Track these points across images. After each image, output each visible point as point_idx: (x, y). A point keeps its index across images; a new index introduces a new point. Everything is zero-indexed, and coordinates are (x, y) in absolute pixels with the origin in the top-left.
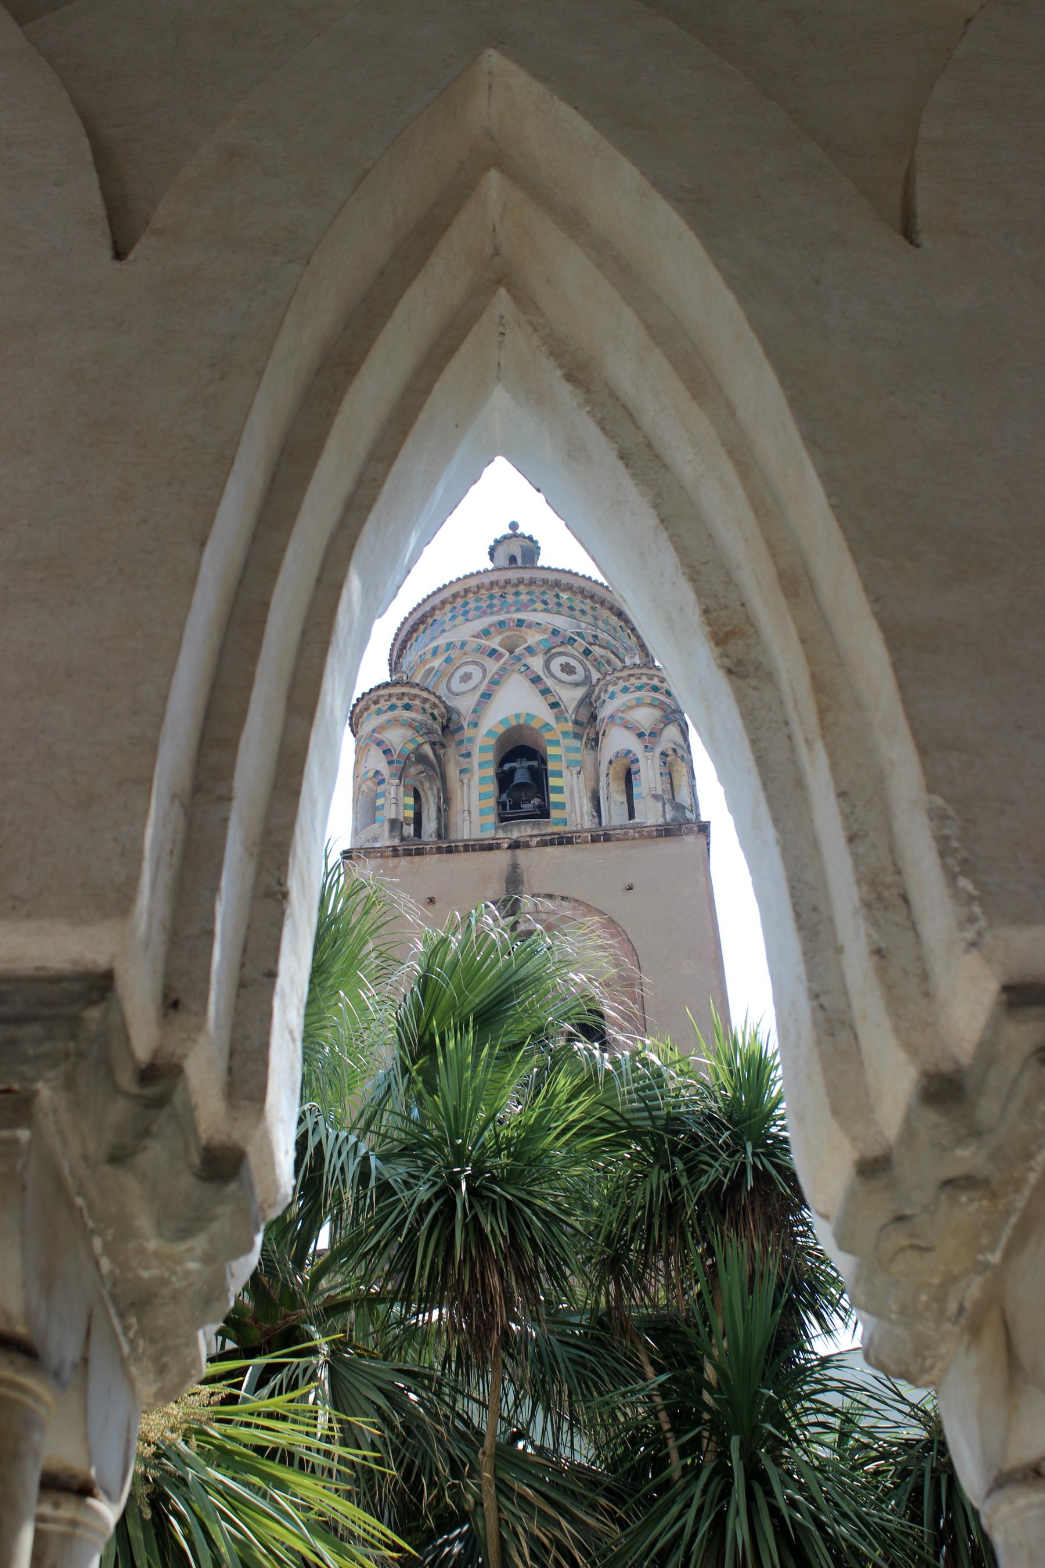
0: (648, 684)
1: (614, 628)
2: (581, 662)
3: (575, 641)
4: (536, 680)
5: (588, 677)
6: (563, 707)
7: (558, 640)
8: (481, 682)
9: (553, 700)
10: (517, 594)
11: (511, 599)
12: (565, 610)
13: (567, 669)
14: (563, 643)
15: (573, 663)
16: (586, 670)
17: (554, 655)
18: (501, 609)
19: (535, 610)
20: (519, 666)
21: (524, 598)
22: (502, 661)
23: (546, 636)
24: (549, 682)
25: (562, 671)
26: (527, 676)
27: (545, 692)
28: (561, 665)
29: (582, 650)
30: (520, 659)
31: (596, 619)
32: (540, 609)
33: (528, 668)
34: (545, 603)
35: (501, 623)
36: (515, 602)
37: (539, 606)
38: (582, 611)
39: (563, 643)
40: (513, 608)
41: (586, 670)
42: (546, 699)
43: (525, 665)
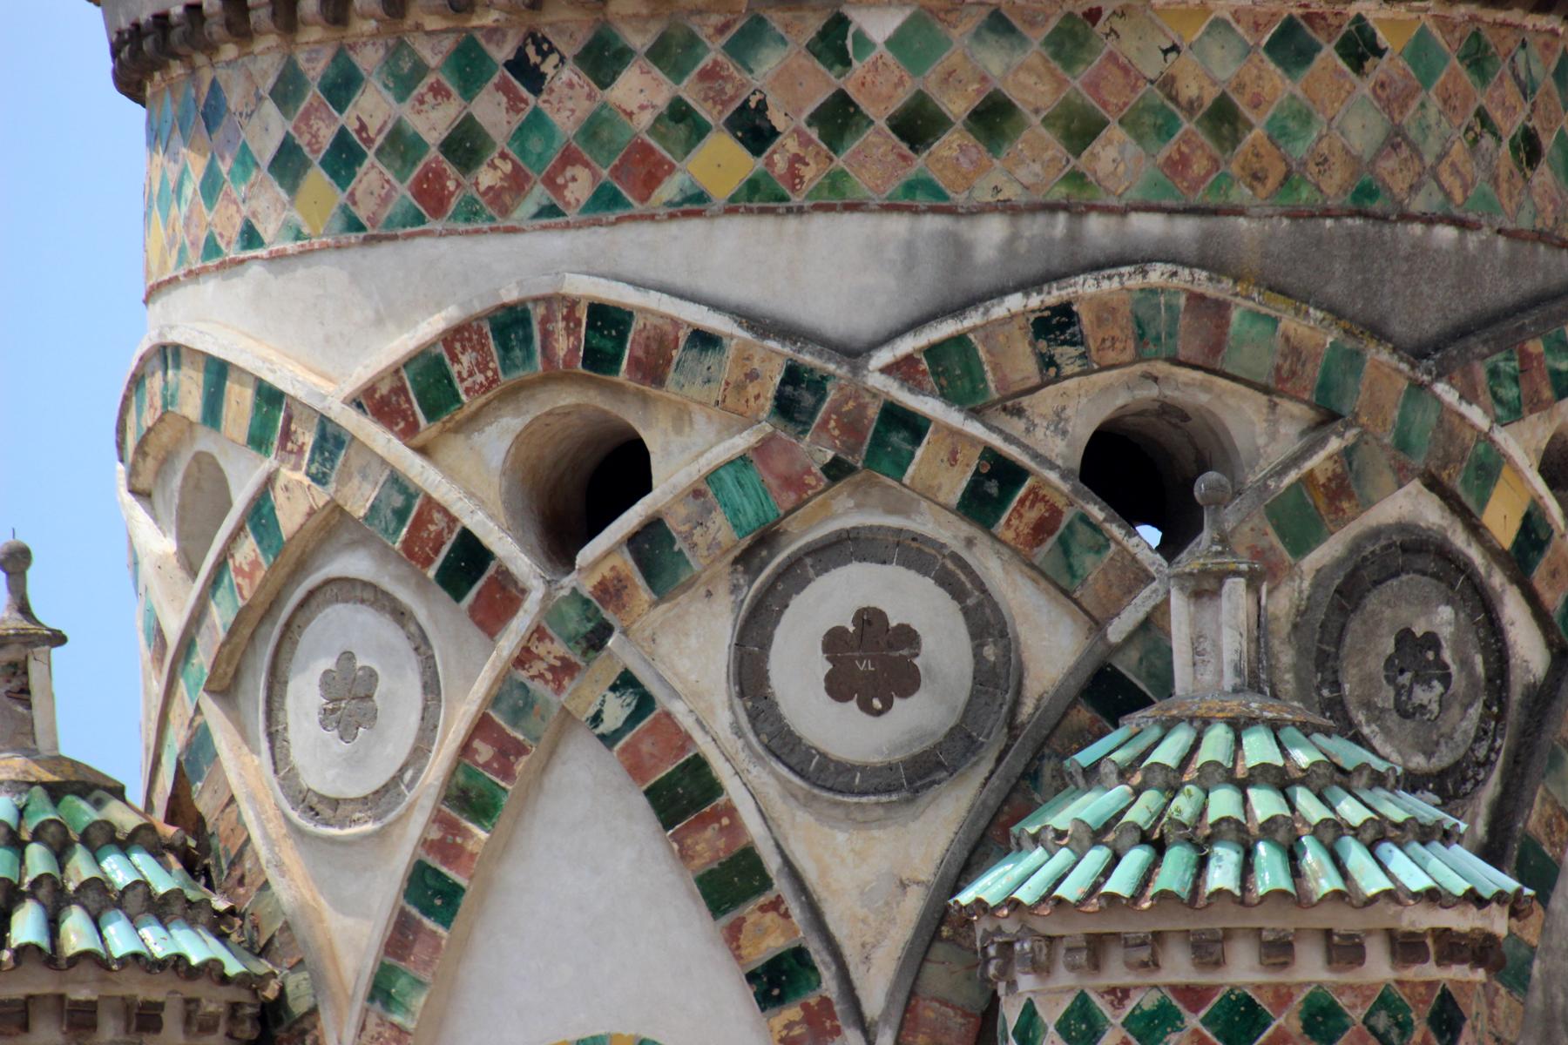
0: (1193, 995)
1: (1223, 118)
2: (956, 580)
3: (915, 426)
4: (683, 796)
5: (997, 675)
6: (829, 986)
7: (817, 450)
8: (419, 753)
9: (770, 943)
10: (603, 60)
11: (568, 98)
12: (873, 155)
13: (871, 661)
14: (837, 471)
15: (909, 598)
16: (986, 622)
17: (793, 576)
18: (518, 182)
19: (694, 204)
20: (592, 692)
21: (639, 92)
22: (510, 640)
23: (742, 442)
24: (748, 786)
25: (838, 688)
26: (635, 769)
27: (732, 884)
28: (834, 642)
29: (955, 485)
30: (597, 638)
31: (1080, 130)
32: (722, 189)
33: (645, 703)
34: (754, 130)
35: (510, 325)
36: (593, 129)
37: (720, 161)
38: (994, 117)
39: (837, 471)
40: (580, 186)
41: (986, 622)
42: (733, 935)
43: (625, 681)
